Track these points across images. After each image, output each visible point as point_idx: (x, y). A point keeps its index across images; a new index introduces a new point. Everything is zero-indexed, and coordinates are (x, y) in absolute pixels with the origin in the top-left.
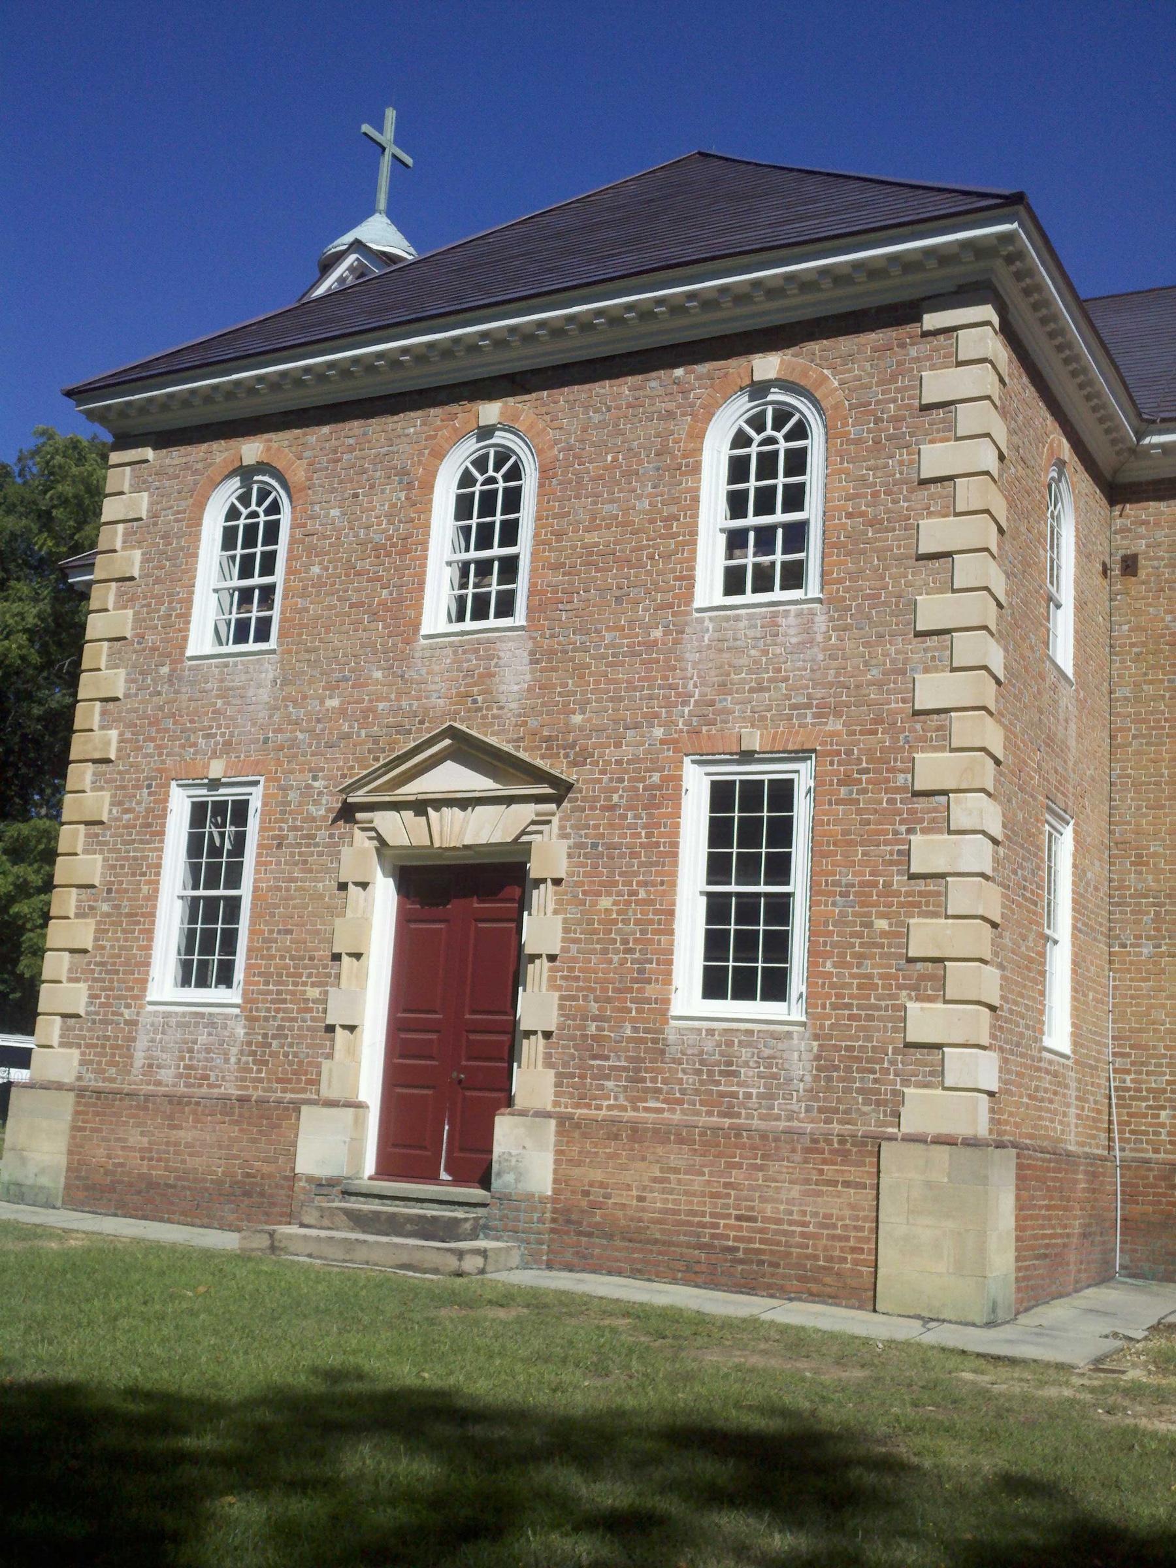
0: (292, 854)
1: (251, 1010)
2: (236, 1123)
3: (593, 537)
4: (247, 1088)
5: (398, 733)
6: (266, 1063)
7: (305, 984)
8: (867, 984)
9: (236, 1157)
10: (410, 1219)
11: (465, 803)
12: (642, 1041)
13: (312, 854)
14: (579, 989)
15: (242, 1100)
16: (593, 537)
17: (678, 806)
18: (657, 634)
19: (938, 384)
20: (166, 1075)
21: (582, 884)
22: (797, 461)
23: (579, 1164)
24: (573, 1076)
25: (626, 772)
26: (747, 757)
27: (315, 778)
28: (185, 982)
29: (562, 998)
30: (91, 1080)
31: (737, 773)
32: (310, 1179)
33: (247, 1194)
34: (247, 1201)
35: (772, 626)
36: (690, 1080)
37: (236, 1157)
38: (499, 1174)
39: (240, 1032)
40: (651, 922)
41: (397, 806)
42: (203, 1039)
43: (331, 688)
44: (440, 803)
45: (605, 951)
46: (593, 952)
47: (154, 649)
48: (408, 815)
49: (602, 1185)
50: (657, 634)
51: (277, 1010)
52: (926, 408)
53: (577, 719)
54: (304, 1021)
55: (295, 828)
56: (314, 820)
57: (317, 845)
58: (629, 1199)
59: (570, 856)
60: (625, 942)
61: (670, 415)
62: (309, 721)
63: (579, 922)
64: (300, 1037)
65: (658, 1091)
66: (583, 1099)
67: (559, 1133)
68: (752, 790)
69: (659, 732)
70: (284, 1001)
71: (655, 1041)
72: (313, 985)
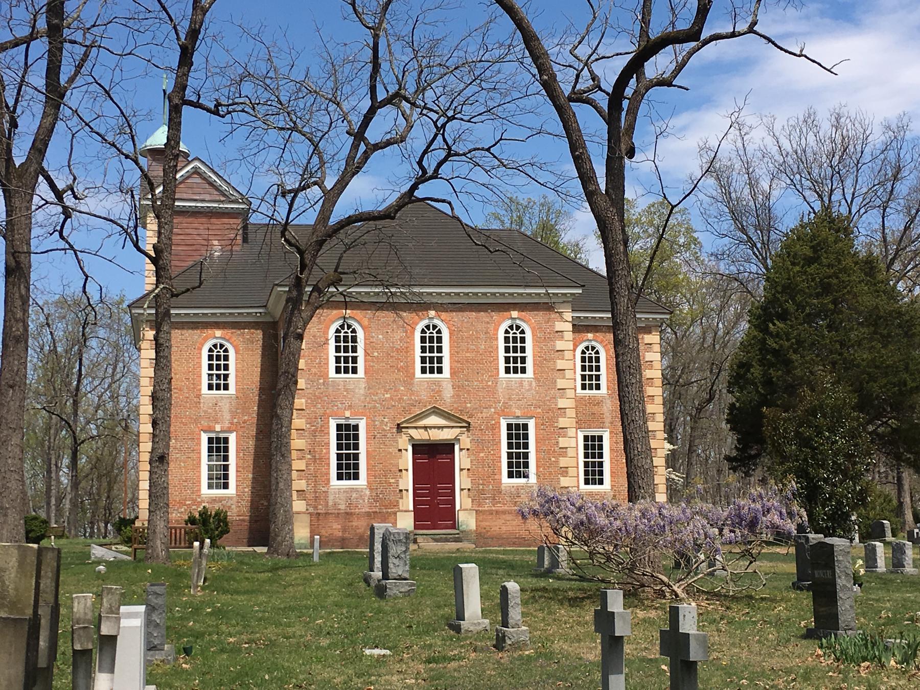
3: (468, 355)
8: (550, 473)
11: (439, 428)
16: (468, 355)
18: (490, 383)
19: (559, 326)
20: (342, 507)
22: (523, 340)
26: (518, 417)
28: (338, 479)
30: (311, 510)
31: (514, 421)
35: (521, 383)
36: (508, 499)
39: (368, 492)
41: (416, 428)
42: (354, 495)
43: (387, 391)
44: (431, 428)
47: (315, 374)
50: (490, 383)
52: (557, 332)
61: (488, 323)
68: (517, 426)
69: (493, 410)
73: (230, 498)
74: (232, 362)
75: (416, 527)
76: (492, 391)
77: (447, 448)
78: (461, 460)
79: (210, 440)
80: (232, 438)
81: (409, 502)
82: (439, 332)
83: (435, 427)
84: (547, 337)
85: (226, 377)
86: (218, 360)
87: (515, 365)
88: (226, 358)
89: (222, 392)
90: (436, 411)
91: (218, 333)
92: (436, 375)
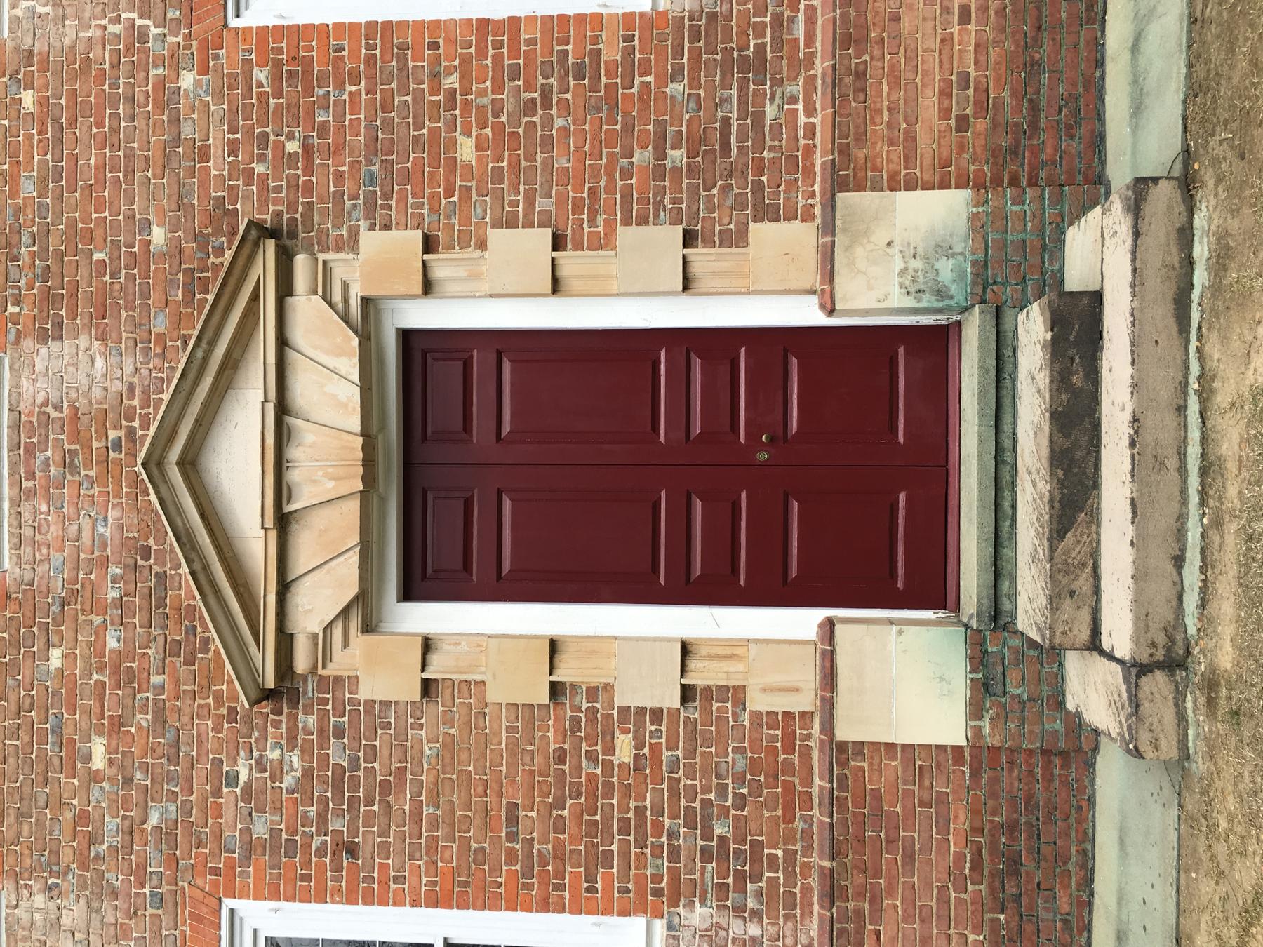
0: (370, 818)
1: (658, 893)
2: (875, 900)
4: (806, 890)
5: (161, 604)
6: (757, 846)
7: (608, 766)
9: (944, 900)
10: (1061, 380)
12: (696, 57)
13: (370, 772)
14: (611, 189)
15: (832, 894)
17: (309, 29)
18: (28, 99)
21: (434, 197)
23: (911, 140)
24: (758, 186)
25: (249, 132)
27: (233, 779)
29: (627, 222)
32: (976, 710)
33: (1015, 863)
34: (1028, 864)
37: (944, 900)
38: (940, 293)
39: (698, 916)
40: (498, 59)
41: (284, 587)
43: (74, 756)
44: (281, 490)
45: (547, 143)
46: (548, 164)
48: (305, 552)
49: (945, 94)
50: (28, 99)
51: (658, 828)
53: (158, 236)
54: (674, 767)
55: (322, 818)
56: (307, 774)
57: (355, 765)
58: (966, 38)
59: (387, 227)
60: (531, 107)
62: (126, 803)
63: (499, 197)
64: (705, 773)
65: (778, 19)
66: (796, 164)
67: (860, 188)
70: (640, 812)
71: (696, 36)
72: (610, 750)
77: (428, 380)
83: (280, 465)
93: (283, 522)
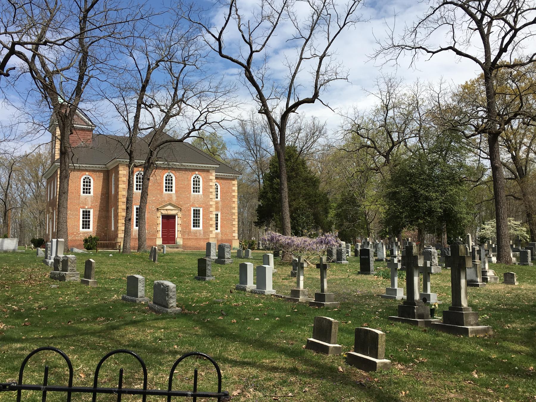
19: (211, 177)
22: (199, 182)
31: (195, 209)
43: (154, 197)
66: (184, 236)
73: (91, 232)
74: (92, 184)
75: (163, 243)
76: (189, 198)
77: (173, 217)
78: (178, 221)
79: (83, 211)
80: (92, 211)
81: (160, 234)
82: (172, 177)
84: (207, 181)
85: (90, 189)
86: (87, 183)
87: (196, 190)
88: (90, 182)
89: (88, 194)
90: (170, 204)
91: (87, 173)
92: (170, 192)
93: (167, 210)
